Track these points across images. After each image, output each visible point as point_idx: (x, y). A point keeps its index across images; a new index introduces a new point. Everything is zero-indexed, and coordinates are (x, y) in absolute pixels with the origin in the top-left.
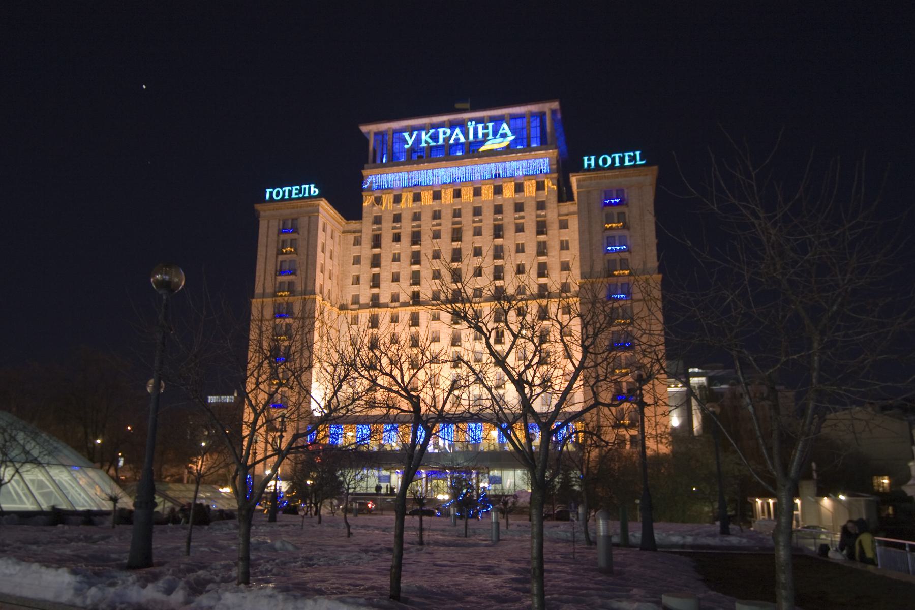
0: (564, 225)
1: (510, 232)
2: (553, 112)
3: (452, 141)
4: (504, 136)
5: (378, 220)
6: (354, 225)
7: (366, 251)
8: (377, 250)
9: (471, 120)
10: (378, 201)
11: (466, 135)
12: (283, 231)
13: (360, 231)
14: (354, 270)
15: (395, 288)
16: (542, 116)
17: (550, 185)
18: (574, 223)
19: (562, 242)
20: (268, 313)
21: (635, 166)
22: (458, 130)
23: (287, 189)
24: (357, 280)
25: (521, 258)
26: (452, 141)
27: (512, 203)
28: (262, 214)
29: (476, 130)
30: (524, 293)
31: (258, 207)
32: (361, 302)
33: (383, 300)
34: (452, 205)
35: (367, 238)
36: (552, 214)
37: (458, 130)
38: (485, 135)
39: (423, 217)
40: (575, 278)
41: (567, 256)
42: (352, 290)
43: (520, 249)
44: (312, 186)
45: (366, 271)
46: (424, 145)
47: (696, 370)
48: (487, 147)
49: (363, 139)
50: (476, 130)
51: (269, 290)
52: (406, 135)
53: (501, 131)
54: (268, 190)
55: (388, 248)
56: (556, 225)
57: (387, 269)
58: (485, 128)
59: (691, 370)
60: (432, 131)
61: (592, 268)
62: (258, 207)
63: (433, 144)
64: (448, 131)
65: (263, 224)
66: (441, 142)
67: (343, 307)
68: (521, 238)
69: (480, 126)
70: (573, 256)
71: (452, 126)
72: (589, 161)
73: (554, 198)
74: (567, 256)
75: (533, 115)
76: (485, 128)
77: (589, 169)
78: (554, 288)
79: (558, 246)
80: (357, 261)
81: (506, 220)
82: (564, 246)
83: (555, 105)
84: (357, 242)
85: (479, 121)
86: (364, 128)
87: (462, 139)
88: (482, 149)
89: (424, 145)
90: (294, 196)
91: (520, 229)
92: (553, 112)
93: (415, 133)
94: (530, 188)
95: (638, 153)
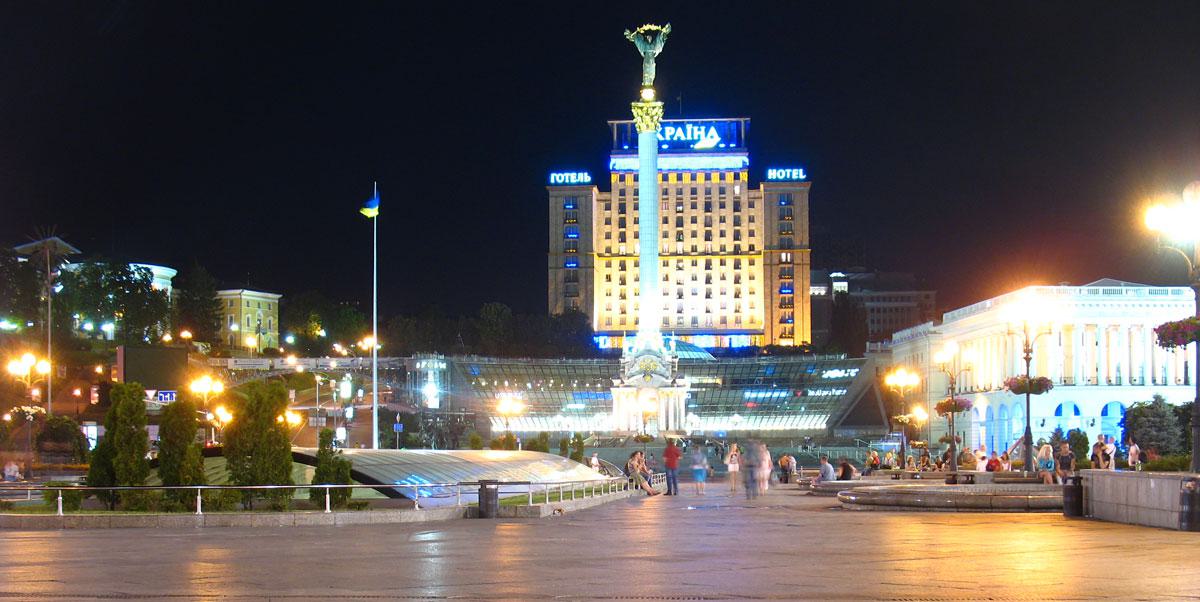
0: (751, 205)
1: (716, 207)
3: (675, 139)
5: (622, 193)
6: (606, 195)
7: (615, 215)
9: (688, 123)
10: (622, 179)
14: (607, 228)
17: (744, 176)
19: (750, 217)
21: (798, 180)
22: (680, 129)
25: (723, 227)
27: (718, 187)
28: (551, 193)
30: (724, 250)
31: (548, 187)
32: (613, 252)
34: (676, 185)
35: (615, 205)
37: (680, 129)
38: (699, 136)
40: (759, 242)
41: (753, 226)
42: (607, 243)
43: (722, 220)
44: (586, 174)
47: (840, 275)
48: (697, 146)
49: (610, 130)
51: (561, 249)
53: (709, 135)
58: (699, 130)
59: (833, 275)
61: (771, 243)
62: (548, 187)
64: (673, 129)
65: (552, 201)
67: (600, 255)
68: (723, 212)
69: (696, 128)
70: (759, 226)
71: (676, 125)
72: (772, 174)
74: (753, 226)
77: (772, 181)
78: (745, 248)
80: (608, 222)
81: (713, 200)
82: (751, 220)
84: (608, 208)
85: (695, 124)
87: (683, 138)
91: (722, 206)
92: (745, 122)
95: (801, 171)
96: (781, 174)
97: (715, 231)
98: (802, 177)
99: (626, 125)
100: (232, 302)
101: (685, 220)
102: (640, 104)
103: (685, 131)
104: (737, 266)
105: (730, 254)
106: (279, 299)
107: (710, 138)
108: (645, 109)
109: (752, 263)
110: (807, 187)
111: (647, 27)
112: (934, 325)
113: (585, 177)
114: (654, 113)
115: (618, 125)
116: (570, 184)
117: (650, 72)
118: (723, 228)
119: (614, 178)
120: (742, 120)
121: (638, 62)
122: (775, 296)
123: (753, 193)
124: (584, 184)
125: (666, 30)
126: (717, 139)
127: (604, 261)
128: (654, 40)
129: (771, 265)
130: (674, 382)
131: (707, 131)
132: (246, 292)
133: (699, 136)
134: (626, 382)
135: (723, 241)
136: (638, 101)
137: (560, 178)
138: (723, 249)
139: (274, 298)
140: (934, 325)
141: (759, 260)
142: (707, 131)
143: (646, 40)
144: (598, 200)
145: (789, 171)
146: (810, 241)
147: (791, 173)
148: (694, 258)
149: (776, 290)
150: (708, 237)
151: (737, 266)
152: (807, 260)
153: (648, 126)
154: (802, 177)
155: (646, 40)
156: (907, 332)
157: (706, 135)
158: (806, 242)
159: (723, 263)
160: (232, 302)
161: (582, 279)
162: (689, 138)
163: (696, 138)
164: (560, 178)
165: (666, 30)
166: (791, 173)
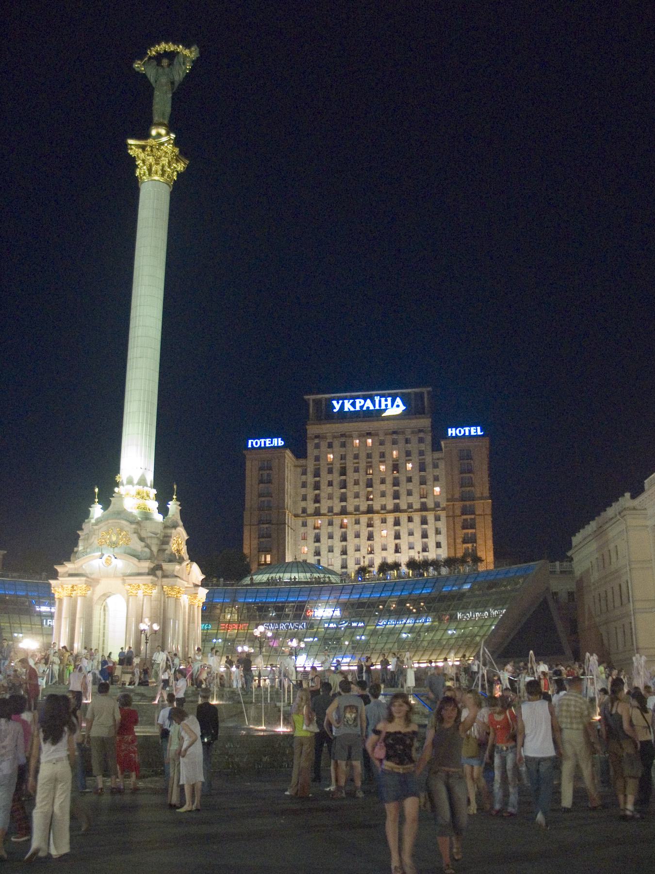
0: (435, 466)
2: (429, 393)
3: (365, 408)
4: (398, 406)
6: (302, 462)
7: (310, 479)
8: (317, 479)
9: (377, 395)
10: (317, 446)
11: (374, 406)
12: (261, 469)
13: (306, 466)
14: (303, 491)
15: (329, 503)
16: (422, 394)
17: (428, 439)
18: (442, 465)
20: (255, 520)
21: (477, 436)
22: (368, 401)
23: (263, 440)
24: (304, 498)
25: (410, 486)
26: (365, 408)
29: (380, 401)
30: (412, 508)
31: (245, 452)
33: (322, 512)
35: (311, 469)
36: (428, 458)
37: (368, 401)
38: (386, 405)
39: (348, 457)
42: (303, 504)
45: (311, 493)
46: (346, 409)
50: (380, 401)
52: (335, 402)
53: (396, 404)
56: (431, 466)
57: (325, 490)
58: (386, 400)
60: (351, 401)
61: (453, 496)
62: (245, 452)
63: (352, 409)
64: (362, 401)
65: (248, 464)
66: (358, 408)
67: (296, 516)
69: (383, 399)
72: (452, 432)
73: (429, 448)
75: (416, 394)
76: (386, 400)
79: (432, 479)
80: (304, 485)
83: (430, 389)
84: (304, 473)
86: (306, 397)
87: (372, 408)
88: (384, 415)
89: (346, 409)
90: (267, 445)
92: (429, 393)
93: (341, 402)
95: (479, 428)
96: (460, 432)
97: (403, 491)
98: (479, 433)
99: (320, 400)
101: (374, 481)
103: (373, 403)
104: (424, 521)
105: (416, 511)
106: (4, 555)
107: (395, 408)
108: (148, 149)
109: (437, 519)
110: (486, 442)
111: (163, 47)
112: (633, 497)
113: (278, 442)
115: (314, 400)
116: (265, 447)
117: (162, 103)
118: (409, 488)
120: (425, 390)
122: (458, 546)
123: (437, 455)
124: (278, 447)
126: (403, 407)
127: (300, 521)
129: (454, 517)
133: (386, 405)
135: (411, 499)
137: (256, 444)
138: (410, 506)
140: (633, 497)
141: (443, 514)
143: (159, 64)
144: (295, 466)
145: (467, 429)
146: (491, 494)
147: (470, 431)
148: (383, 516)
149: (459, 541)
150: (396, 496)
151: (424, 521)
152: (489, 511)
153: (150, 170)
154: (479, 433)
156: (593, 526)
157: (392, 406)
158: (486, 493)
159: (410, 520)
161: (274, 535)
162: (377, 407)
163: (383, 407)
164: (256, 444)
166: (470, 431)
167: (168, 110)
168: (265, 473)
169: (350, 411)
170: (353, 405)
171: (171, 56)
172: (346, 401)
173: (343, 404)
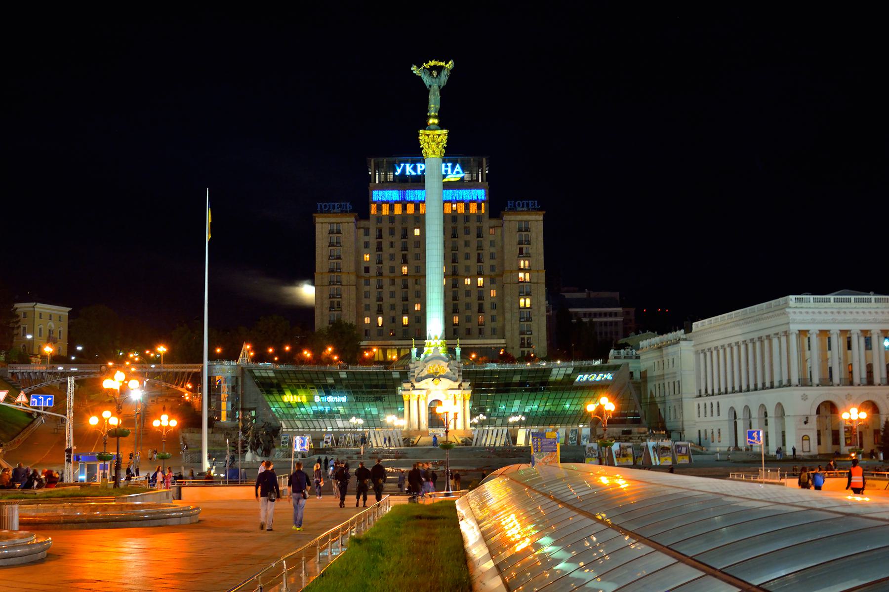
6: (363, 223)
10: (379, 208)
12: (331, 232)
25: (468, 250)
35: (373, 232)
38: (446, 171)
46: (408, 173)
51: (326, 270)
53: (456, 170)
54: (319, 204)
55: (386, 239)
63: (413, 173)
66: (419, 173)
76: (447, 166)
89: (408, 173)
93: (402, 165)
94: (473, 208)
100: (25, 314)
102: (428, 132)
111: (432, 63)
114: (439, 140)
117: (434, 104)
119: (373, 210)
121: (425, 92)
125: (450, 65)
128: (439, 74)
130: (460, 385)
131: (453, 168)
132: (39, 305)
133: (446, 171)
134: (417, 385)
136: (425, 129)
139: (64, 311)
142: (453, 168)
143: (431, 74)
155: (431, 74)
157: (452, 171)
160: (25, 314)
165: (450, 65)
167: (438, 106)
168: (335, 236)
169: (411, 175)
170: (415, 169)
171: (439, 69)
172: (408, 165)
173: (404, 168)
